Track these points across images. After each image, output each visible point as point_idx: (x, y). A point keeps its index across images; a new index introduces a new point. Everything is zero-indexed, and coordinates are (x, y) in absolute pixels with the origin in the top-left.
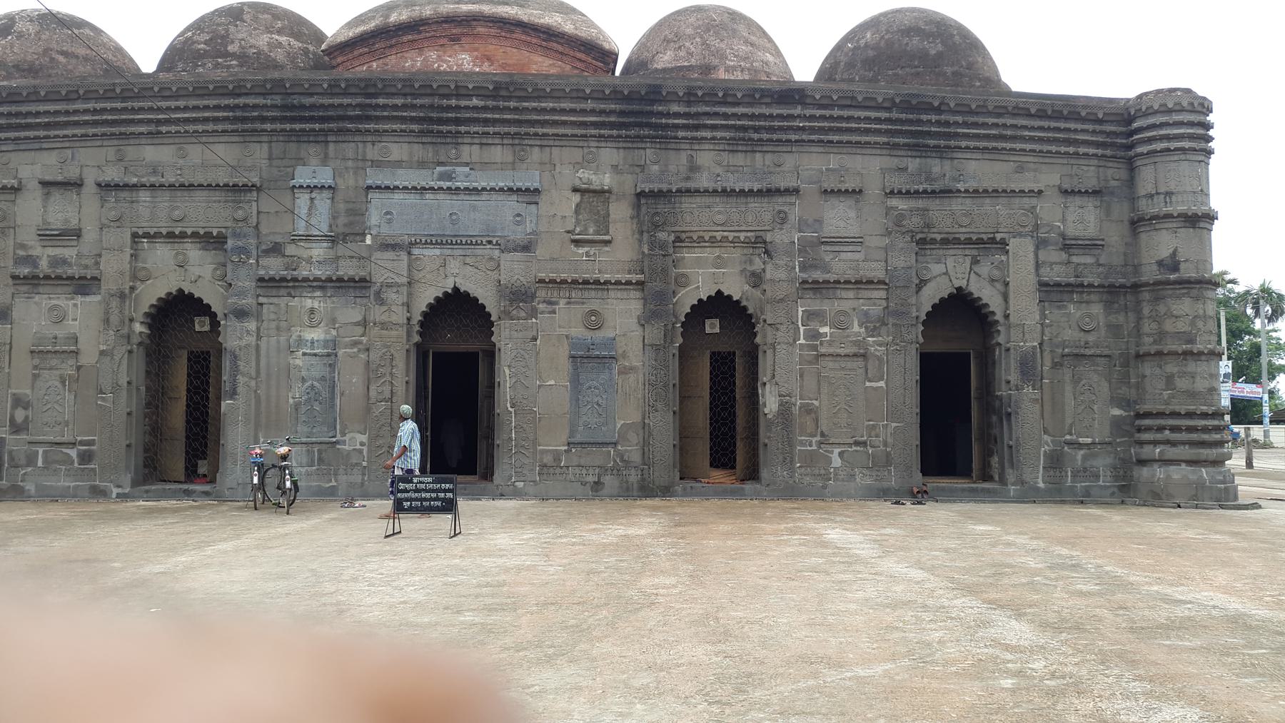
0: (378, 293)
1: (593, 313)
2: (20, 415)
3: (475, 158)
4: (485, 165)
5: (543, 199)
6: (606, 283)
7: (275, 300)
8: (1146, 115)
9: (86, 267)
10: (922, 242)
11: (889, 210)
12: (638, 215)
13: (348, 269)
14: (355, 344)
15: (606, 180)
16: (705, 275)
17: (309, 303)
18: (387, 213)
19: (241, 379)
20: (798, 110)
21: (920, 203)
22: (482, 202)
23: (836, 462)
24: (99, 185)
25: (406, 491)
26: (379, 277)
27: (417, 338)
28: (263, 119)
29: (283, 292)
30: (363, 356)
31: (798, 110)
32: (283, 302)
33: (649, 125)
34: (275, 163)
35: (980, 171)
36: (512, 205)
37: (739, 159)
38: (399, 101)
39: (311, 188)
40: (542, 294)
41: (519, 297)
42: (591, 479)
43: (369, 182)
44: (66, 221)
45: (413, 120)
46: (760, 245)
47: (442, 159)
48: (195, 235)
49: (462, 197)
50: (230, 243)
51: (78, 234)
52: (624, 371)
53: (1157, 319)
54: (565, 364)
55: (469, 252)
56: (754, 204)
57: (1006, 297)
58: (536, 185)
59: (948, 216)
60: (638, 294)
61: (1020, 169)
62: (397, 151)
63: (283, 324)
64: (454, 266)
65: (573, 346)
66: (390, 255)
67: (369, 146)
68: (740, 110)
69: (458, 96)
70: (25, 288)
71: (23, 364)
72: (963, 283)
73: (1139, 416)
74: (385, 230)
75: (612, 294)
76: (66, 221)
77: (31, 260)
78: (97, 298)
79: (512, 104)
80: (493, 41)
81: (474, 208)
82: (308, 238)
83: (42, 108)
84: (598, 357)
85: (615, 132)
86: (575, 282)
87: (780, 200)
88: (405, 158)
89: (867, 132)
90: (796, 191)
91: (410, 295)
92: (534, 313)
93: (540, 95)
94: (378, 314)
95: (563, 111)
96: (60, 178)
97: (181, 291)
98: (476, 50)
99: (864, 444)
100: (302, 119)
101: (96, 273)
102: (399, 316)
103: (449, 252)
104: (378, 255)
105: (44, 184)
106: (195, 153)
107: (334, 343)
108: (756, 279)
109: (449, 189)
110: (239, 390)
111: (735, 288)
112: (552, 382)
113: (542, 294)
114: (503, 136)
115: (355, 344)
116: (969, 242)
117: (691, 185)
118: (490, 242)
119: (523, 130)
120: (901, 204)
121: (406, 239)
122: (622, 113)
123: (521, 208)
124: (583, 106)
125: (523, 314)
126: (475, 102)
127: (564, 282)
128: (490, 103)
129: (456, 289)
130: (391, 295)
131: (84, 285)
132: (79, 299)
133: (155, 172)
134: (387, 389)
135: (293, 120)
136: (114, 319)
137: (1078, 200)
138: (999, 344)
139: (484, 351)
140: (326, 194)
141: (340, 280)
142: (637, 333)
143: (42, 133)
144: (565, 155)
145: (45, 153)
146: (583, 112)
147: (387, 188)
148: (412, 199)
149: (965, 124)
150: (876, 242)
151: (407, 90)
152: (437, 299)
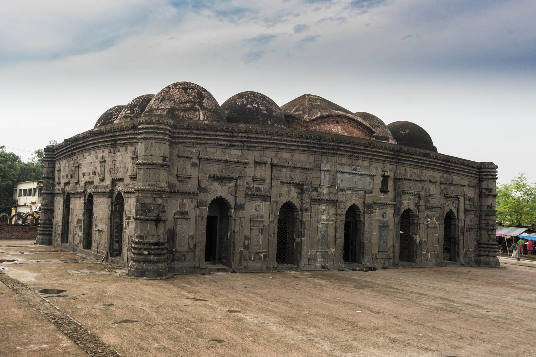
5: (375, 178)
7: (315, 206)
8: (486, 168)
9: (266, 192)
10: (446, 197)
11: (441, 188)
13: (332, 197)
15: (388, 174)
16: (407, 203)
17: (323, 207)
19: (306, 231)
20: (426, 159)
21: (446, 186)
22: (362, 178)
23: (429, 256)
24: (272, 165)
26: (339, 200)
28: (313, 147)
29: (317, 203)
31: (426, 159)
33: (398, 159)
34: (316, 161)
35: (456, 179)
36: (368, 179)
37: (415, 171)
38: (345, 145)
39: (325, 171)
41: (369, 207)
42: (383, 262)
44: (261, 176)
45: (349, 152)
46: (419, 196)
48: (293, 183)
50: (304, 187)
52: (390, 230)
54: (377, 227)
56: (418, 184)
57: (458, 212)
59: (453, 190)
60: (393, 208)
61: (462, 179)
62: (344, 161)
63: (317, 214)
65: (380, 222)
66: (342, 193)
68: (415, 157)
70: (249, 198)
71: (247, 225)
72: (451, 208)
73: (480, 244)
76: (261, 176)
78: (269, 203)
81: (361, 180)
82: (324, 187)
83: (257, 136)
87: (423, 183)
89: (439, 166)
90: (425, 181)
92: (372, 212)
96: (262, 161)
97: (289, 201)
99: (434, 251)
100: (324, 149)
101: (269, 195)
104: (339, 193)
105: (256, 163)
106: (296, 156)
107: (328, 220)
108: (417, 205)
110: (306, 234)
111: (412, 207)
115: (333, 220)
116: (453, 197)
117: (406, 177)
120: (443, 186)
122: (391, 154)
126: (361, 147)
128: (366, 148)
130: (342, 206)
131: (266, 198)
132: (264, 203)
133: (286, 162)
135: (322, 148)
136: (274, 210)
137: (471, 188)
138: (455, 224)
140: (327, 173)
141: (332, 200)
142: (393, 219)
143: (257, 145)
149: (454, 166)
150: (439, 196)
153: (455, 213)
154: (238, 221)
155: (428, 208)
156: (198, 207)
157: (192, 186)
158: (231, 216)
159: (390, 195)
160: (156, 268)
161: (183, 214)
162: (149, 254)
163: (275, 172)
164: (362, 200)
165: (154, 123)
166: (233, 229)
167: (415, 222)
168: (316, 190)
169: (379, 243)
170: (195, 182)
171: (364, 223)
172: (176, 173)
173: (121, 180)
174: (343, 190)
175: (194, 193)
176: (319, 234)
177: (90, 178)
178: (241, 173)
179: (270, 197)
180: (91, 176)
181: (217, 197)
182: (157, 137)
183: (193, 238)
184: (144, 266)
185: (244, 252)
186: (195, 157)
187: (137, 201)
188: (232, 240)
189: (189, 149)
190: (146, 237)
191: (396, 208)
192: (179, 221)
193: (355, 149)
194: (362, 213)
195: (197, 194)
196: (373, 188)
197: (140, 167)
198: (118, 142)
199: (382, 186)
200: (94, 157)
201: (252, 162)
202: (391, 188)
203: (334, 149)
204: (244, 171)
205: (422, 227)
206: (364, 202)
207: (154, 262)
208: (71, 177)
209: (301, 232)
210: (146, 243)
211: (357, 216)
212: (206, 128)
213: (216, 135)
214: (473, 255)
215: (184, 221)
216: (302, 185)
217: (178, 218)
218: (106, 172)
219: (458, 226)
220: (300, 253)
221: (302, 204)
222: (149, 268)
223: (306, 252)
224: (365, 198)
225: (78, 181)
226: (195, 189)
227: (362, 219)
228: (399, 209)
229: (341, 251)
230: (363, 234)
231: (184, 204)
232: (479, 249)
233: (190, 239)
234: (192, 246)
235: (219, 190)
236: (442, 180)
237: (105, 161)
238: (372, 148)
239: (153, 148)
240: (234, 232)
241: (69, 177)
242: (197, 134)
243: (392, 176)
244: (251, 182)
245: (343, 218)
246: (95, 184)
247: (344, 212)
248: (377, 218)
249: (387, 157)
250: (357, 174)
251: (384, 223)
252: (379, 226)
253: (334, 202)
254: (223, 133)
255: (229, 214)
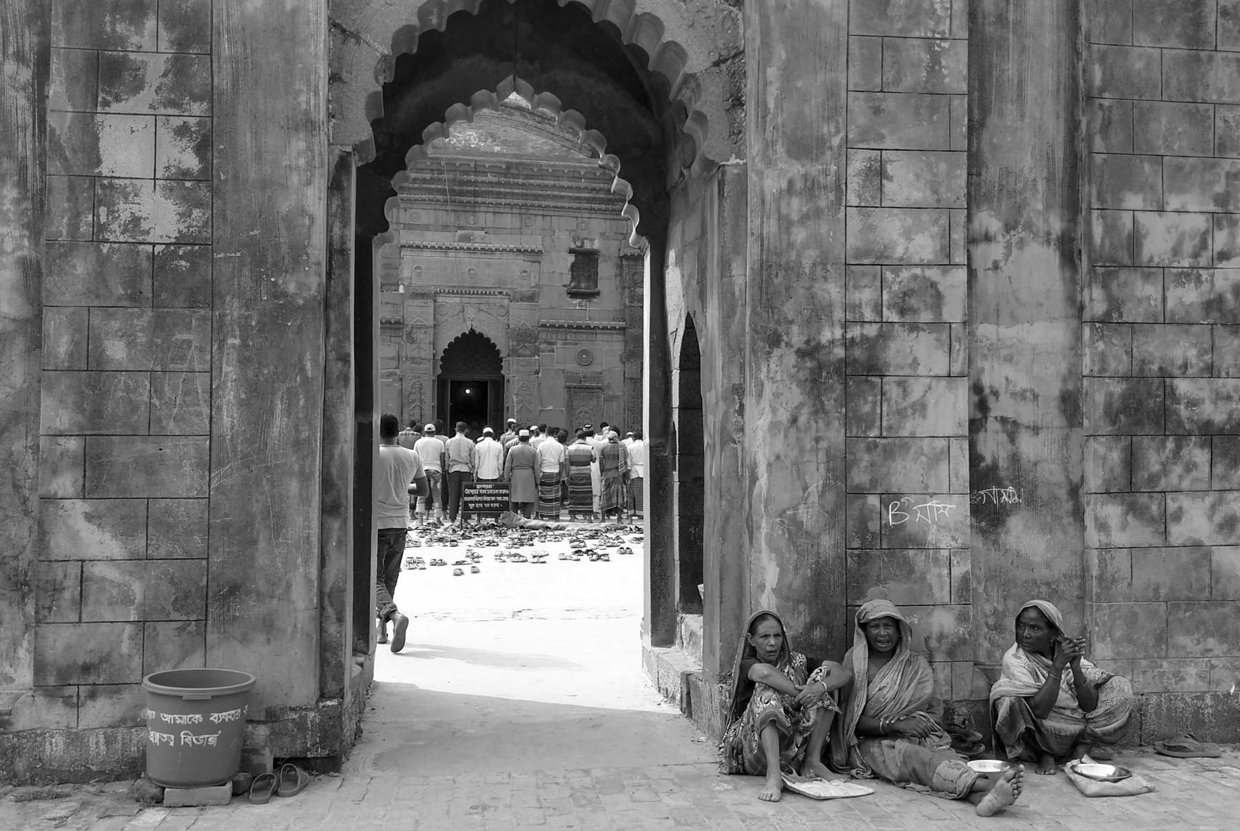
0: (409, 334)
1: (584, 352)
3: (489, 224)
4: (497, 230)
5: (545, 260)
6: (595, 328)
12: (621, 274)
14: (390, 375)
18: (417, 268)
22: (495, 259)
25: (471, 495)
26: (410, 321)
27: (440, 372)
30: (397, 385)
36: (520, 263)
40: (543, 336)
43: (403, 242)
47: (462, 224)
49: (478, 255)
55: (483, 301)
58: (540, 247)
60: (620, 338)
64: (470, 312)
65: (568, 379)
66: (419, 302)
67: (402, 211)
69: (476, 172)
74: (415, 282)
79: (520, 181)
80: (497, 121)
81: (489, 265)
84: (588, 388)
85: (603, 206)
86: (570, 327)
88: (432, 222)
91: (435, 334)
92: (537, 351)
93: (542, 174)
94: (409, 350)
95: (561, 188)
98: (482, 128)
102: (427, 352)
103: (465, 300)
104: (410, 302)
109: (469, 249)
112: (551, 408)
113: (543, 336)
114: (512, 206)
115: (390, 375)
118: (501, 293)
119: (529, 202)
121: (433, 290)
123: (527, 266)
124: (578, 184)
125: (528, 352)
126: (490, 178)
127: (562, 327)
128: (503, 180)
129: (472, 331)
130: (420, 335)
134: (417, 411)
139: (492, 381)
142: (619, 368)
146: (578, 189)
147: (418, 247)
148: (437, 256)
151: (434, 167)
152: (457, 339)
164: (503, 320)
174: (423, 296)
193: (462, 183)
196: (537, 286)
199: (573, 278)
238: (528, 177)
249: (589, 200)
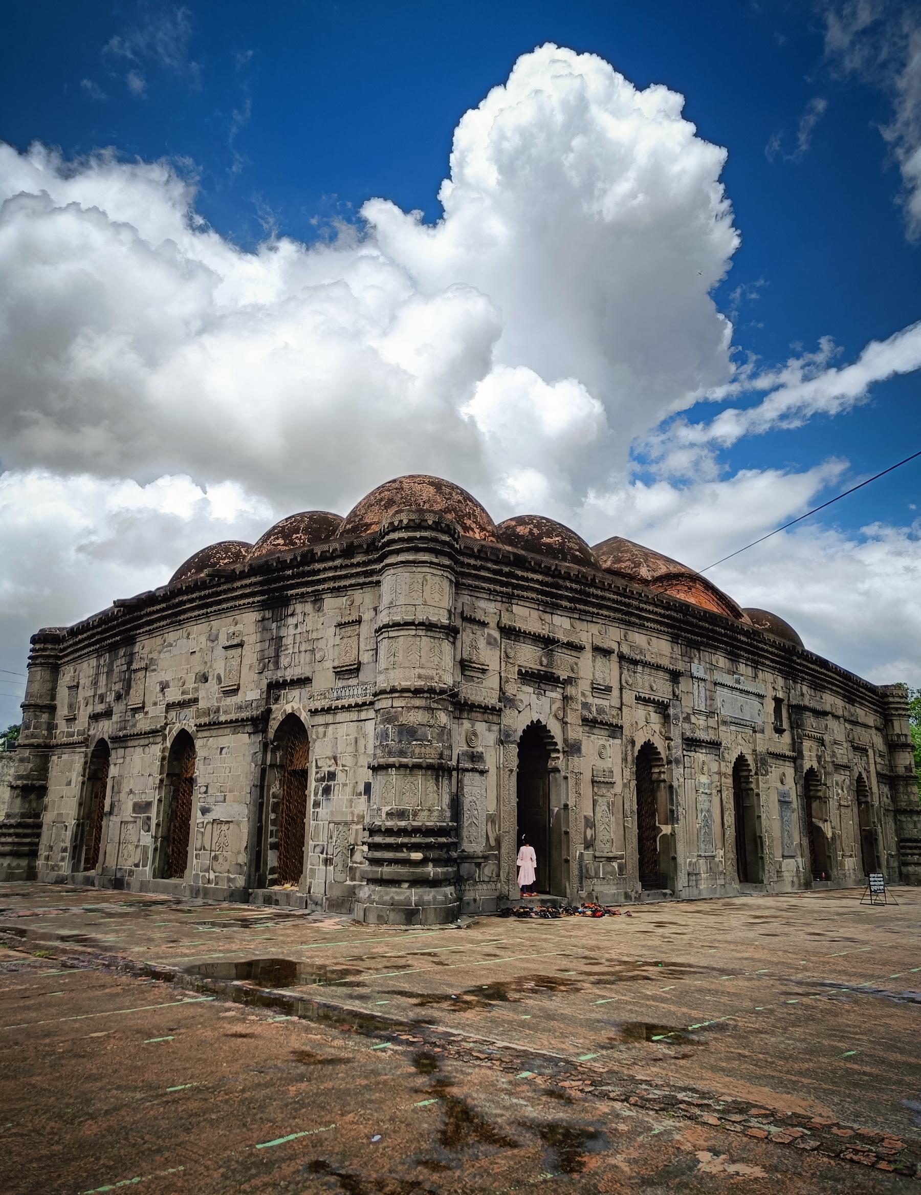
2: (589, 832)
7: (688, 753)
8: (893, 696)
10: (852, 746)
15: (780, 695)
19: (680, 809)
24: (622, 657)
32: (692, 754)
36: (755, 702)
40: (770, 760)
43: (720, 680)
46: (821, 742)
48: (654, 702)
50: (671, 711)
51: (609, 689)
53: (908, 794)
62: (722, 661)
70: (587, 728)
71: (587, 789)
75: (787, 763)
77: (586, 705)
78: (618, 741)
92: (767, 774)
96: (605, 646)
103: (738, 729)
105: (597, 649)
110: (681, 817)
120: (848, 726)
130: (726, 755)
131: (615, 730)
136: (630, 758)
140: (702, 684)
143: (595, 610)
144: (769, 677)
145: (593, 625)
150: (845, 744)
153: (866, 779)
154: (571, 782)
155: (838, 767)
156: (501, 742)
157: (484, 692)
158: (556, 770)
159: (786, 738)
160: (440, 898)
161: (476, 757)
162: (424, 862)
163: (625, 672)
165: (429, 528)
166: (563, 803)
167: (820, 794)
168: (687, 719)
169: (782, 837)
170: (492, 681)
171: (758, 795)
172: (458, 658)
173: (303, 682)
175: (494, 709)
176: (699, 815)
177: (183, 693)
178: (572, 670)
179: (621, 727)
180: (190, 685)
181: (532, 721)
182: (435, 560)
183: (493, 822)
184: (413, 895)
185: (586, 858)
186: (493, 625)
187: (389, 718)
188: (564, 829)
189: (482, 604)
190: (415, 814)
191: (797, 769)
192: (467, 774)
194: (754, 772)
195: (500, 710)
197: (392, 634)
198: (290, 592)
200: (203, 639)
201: (588, 647)
202: (785, 725)
203: (709, 638)
204: (576, 664)
205: (833, 804)
206: (754, 751)
207: (434, 883)
208: (118, 698)
209: (672, 811)
210: (416, 831)
211: (742, 780)
212: (512, 559)
213: (526, 579)
214: (896, 864)
215: (477, 774)
216: (666, 707)
217: (467, 770)
218: (245, 670)
219: (873, 806)
220: (674, 859)
221: (669, 748)
222: (426, 898)
223: (685, 856)
224: (755, 742)
225: (144, 703)
226: (492, 700)
227: (753, 786)
228: (801, 766)
229: (732, 855)
230: (759, 817)
231: (475, 734)
232: (902, 851)
233: (489, 824)
234: (493, 843)
235: (536, 707)
236: (846, 714)
237: (241, 645)
239: (427, 588)
240: (566, 806)
241: (110, 698)
242: (495, 572)
243: (786, 702)
244: (588, 693)
245: (730, 781)
246: (202, 704)
247: (730, 771)
248: (774, 785)
250: (741, 691)
251: (784, 795)
252: (779, 801)
253: (714, 745)
254: (540, 577)
255: (551, 764)
